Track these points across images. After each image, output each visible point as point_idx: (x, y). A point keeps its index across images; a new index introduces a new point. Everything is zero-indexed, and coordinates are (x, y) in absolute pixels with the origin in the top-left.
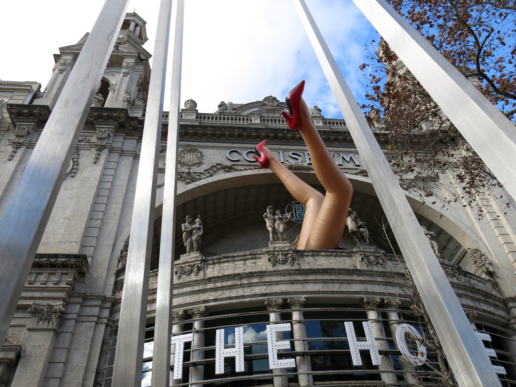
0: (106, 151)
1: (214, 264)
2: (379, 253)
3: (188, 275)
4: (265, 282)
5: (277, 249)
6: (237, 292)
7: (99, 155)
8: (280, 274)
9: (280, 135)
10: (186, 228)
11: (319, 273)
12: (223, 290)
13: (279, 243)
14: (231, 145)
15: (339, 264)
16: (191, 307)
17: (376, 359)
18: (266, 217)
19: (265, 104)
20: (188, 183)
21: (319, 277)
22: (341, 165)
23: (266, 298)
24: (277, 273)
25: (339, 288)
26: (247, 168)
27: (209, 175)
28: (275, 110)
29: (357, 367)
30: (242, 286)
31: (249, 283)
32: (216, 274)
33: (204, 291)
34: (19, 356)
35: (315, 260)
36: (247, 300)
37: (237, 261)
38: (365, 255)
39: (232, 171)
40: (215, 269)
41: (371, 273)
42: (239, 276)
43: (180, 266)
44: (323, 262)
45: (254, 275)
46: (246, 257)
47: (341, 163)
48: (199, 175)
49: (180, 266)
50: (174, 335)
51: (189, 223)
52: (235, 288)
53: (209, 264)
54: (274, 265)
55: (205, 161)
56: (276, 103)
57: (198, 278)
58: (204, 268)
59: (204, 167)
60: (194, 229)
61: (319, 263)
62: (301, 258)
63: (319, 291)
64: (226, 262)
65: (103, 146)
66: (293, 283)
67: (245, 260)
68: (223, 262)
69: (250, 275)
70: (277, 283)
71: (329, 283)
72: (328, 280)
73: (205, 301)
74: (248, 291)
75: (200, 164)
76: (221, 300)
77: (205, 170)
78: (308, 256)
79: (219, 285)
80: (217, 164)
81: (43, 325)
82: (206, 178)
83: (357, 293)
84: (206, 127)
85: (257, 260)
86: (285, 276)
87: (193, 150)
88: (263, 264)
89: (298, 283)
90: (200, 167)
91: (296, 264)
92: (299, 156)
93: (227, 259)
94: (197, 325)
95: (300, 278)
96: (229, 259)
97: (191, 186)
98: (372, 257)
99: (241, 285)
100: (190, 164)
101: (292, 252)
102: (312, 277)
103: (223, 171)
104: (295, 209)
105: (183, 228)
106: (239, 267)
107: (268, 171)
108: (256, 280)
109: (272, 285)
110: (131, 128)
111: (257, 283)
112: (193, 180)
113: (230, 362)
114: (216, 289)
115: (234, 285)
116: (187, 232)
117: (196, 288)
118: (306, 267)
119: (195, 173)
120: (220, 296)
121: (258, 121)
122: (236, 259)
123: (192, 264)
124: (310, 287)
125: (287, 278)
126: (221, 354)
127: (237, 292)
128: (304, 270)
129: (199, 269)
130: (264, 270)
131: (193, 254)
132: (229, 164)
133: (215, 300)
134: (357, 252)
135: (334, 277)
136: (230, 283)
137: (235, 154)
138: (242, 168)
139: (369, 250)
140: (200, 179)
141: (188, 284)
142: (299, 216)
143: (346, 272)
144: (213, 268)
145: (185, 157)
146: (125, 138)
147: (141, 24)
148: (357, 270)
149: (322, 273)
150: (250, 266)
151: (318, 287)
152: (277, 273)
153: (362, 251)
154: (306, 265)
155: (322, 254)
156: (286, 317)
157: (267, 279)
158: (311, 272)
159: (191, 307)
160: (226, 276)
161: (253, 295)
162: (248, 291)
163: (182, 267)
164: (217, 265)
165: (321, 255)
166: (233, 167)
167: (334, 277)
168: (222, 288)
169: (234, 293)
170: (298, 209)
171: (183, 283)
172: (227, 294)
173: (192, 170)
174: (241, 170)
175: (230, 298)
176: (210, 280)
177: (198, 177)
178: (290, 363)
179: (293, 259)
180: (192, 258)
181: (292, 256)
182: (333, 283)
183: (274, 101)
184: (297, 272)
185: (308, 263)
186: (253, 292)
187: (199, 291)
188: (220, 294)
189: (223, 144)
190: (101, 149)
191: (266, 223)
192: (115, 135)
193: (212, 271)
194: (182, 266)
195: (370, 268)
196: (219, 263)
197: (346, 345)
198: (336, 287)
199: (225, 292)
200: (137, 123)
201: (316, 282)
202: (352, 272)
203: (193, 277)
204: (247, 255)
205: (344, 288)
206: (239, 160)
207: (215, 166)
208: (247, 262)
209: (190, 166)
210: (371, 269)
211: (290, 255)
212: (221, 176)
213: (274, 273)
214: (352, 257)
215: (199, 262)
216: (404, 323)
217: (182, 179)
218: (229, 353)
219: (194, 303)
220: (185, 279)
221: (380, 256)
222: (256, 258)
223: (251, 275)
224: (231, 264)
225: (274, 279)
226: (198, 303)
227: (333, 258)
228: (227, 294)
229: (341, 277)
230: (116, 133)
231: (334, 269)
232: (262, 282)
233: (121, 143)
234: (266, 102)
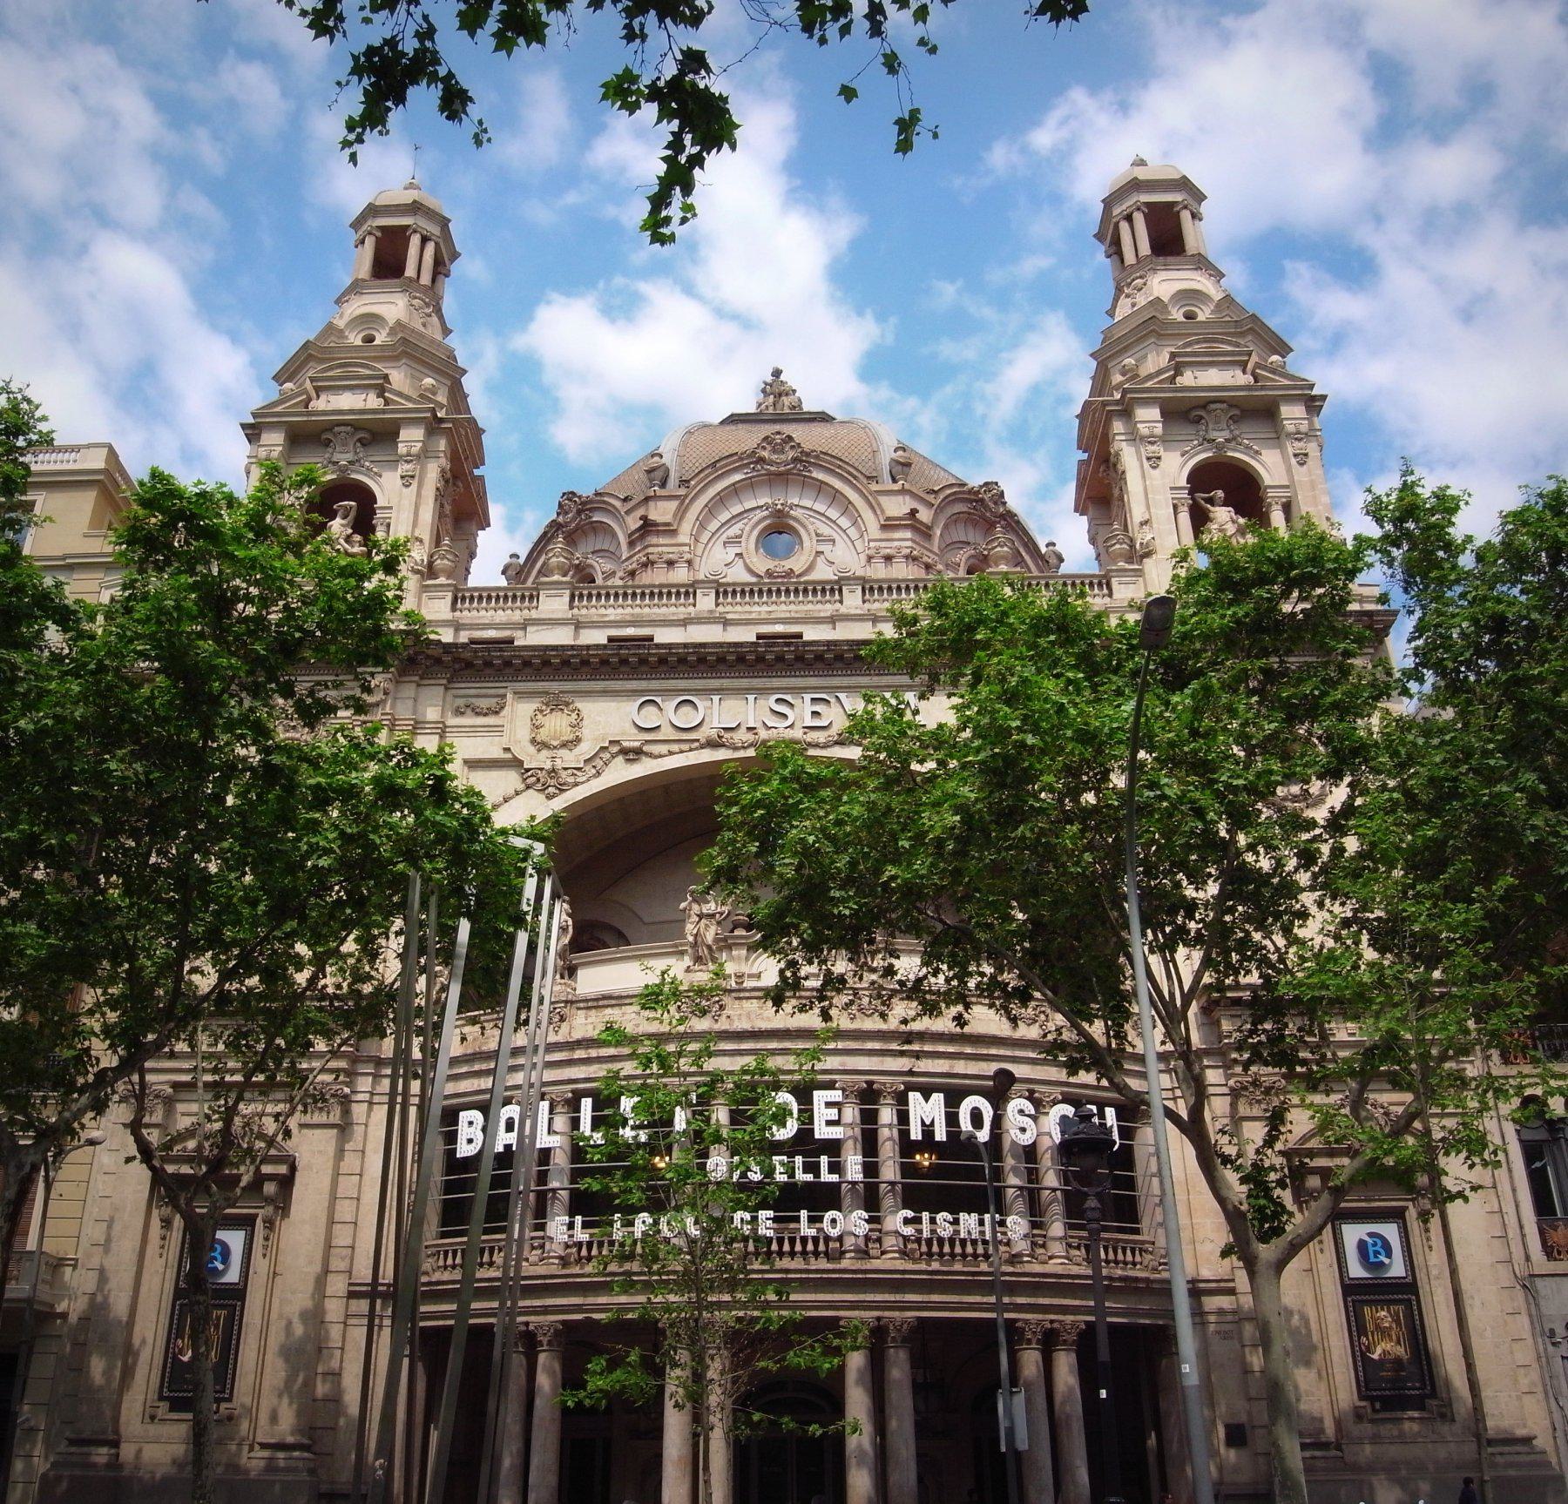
14: (643, 685)
19: (762, 460)
20: (550, 797)
26: (675, 747)
28: (788, 473)
34: (293, 1169)
59: (586, 749)
79: (593, 1053)
81: (319, 1118)
90: (577, 750)
91: (723, 1018)
97: (560, 803)
103: (620, 758)
129: (562, 1019)
137: (651, 709)
138: (663, 749)
140: (576, 784)
147: (434, 229)
166: (645, 748)
173: (559, 764)
212: (620, 773)
217: (539, 786)
233: (410, 703)
234: (765, 454)
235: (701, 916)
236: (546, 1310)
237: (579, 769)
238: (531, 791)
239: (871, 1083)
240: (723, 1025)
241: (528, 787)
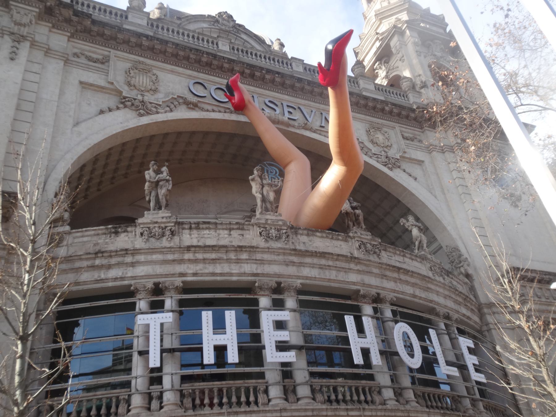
0: (28, 44)
1: (190, 228)
2: (376, 241)
3: (158, 239)
4: (256, 260)
6: (222, 267)
7: (17, 49)
8: (274, 252)
9: (258, 74)
10: (150, 177)
11: (316, 256)
12: (205, 263)
13: (270, 214)
14: (195, 74)
15: (336, 249)
16: (163, 280)
17: (376, 359)
18: (253, 180)
20: (141, 115)
21: (315, 261)
22: (323, 127)
23: (257, 279)
24: (270, 250)
25: (336, 276)
27: (168, 109)
29: (357, 366)
31: (238, 259)
32: (195, 242)
33: (181, 261)
35: (311, 241)
36: (235, 278)
37: (219, 229)
39: (197, 109)
40: (193, 236)
41: (368, 263)
42: (225, 249)
43: (145, 226)
44: (320, 243)
45: (244, 250)
46: (232, 226)
47: (323, 125)
48: (155, 107)
49: (145, 226)
50: (142, 313)
51: (154, 171)
52: (220, 263)
53: (183, 229)
54: (266, 241)
55: (161, 89)
56: (232, 24)
57: (172, 244)
58: (179, 233)
60: (161, 180)
61: (315, 245)
62: (294, 236)
63: (315, 278)
64: (207, 228)
65: (22, 36)
66: (287, 265)
67: (230, 230)
68: (203, 229)
69: (238, 249)
70: (270, 262)
71: (326, 269)
72: (325, 265)
73: (182, 274)
74: (235, 269)
75: (155, 91)
76: (202, 275)
77: (163, 102)
78: (302, 234)
79: (200, 256)
80: (178, 96)
82: (166, 112)
83: (354, 283)
84: (167, 42)
86: (278, 255)
87: (146, 71)
88: (252, 237)
89: (293, 265)
90: (156, 96)
92: (277, 105)
93: (207, 226)
94: (168, 303)
95: (295, 259)
96: (211, 226)
97: (145, 120)
98: (369, 245)
99: (227, 259)
100: (143, 89)
102: (308, 260)
103: (184, 107)
105: (147, 177)
106: (223, 237)
107: (242, 118)
109: (263, 264)
110: (60, 18)
111: (246, 259)
112: (148, 113)
113: (220, 350)
114: (196, 261)
115: (218, 259)
116: (152, 182)
117: (170, 257)
118: (301, 247)
119: (151, 103)
120: (201, 270)
121: (227, 48)
122: (219, 227)
123: (163, 225)
125: (281, 258)
126: (209, 340)
128: (300, 251)
129: (173, 233)
131: (162, 213)
132: (195, 100)
133: (195, 274)
134: (354, 237)
135: (330, 263)
136: (213, 256)
137: (200, 87)
138: (210, 108)
139: (366, 237)
140: (158, 113)
141: (159, 250)
143: (344, 258)
144: (190, 235)
145: (136, 78)
146: (50, 31)
148: (355, 258)
149: (320, 256)
150: (234, 238)
153: (359, 237)
154: (302, 245)
155: (318, 234)
156: (278, 305)
157: (259, 256)
158: (308, 254)
159: (163, 280)
160: (209, 246)
161: (242, 273)
162: (235, 269)
163: (149, 228)
164: (195, 232)
165: (316, 236)
166: (199, 105)
167: (330, 263)
169: (218, 269)
170: (271, 172)
171: (152, 249)
172: (210, 268)
173: (146, 99)
174: (208, 111)
175: (213, 274)
176: (188, 248)
177: (154, 110)
178: (289, 356)
179: (288, 236)
180: (163, 218)
181: (286, 233)
182: (330, 269)
183: (230, 20)
184: (293, 252)
185: (304, 243)
186: (242, 271)
187: (174, 261)
189: (184, 70)
190: (19, 39)
191: (251, 187)
192: (36, 23)
193: (189, 238)
194: (148, 226)
195: (366, 257)
196: (198, 228)
197: (346, 340)
198: (332, 275)
199: (207, 266)
200: (71, 13)
201: (312, 266)
202: (350, 259)
203: (165, 243)
204: (233, 224)
205: (341, 276)
206: (205, 97)
207: (175, 99)
208: (232, 232)
209: (142, 91)
210: (368, 258)
211: (284, 231)
212: (182, 114)
214: (348, 242)
215: (173, 224)
216: (402, 321)
218: (220, 340)
219: (166, 276)
220: (154, 243)
221: (376, 245)
222: (243, 229)
223: (240, 248)
224: (212, 232)
226: (173, 275)
227: (329, 240)
228: (210, 268)
229: (338, 264)
230: (39, 20)
231: (332, 254)
232: (253, 259)
237: (160, 105)
238: (127, 109)
241: (125, 107)
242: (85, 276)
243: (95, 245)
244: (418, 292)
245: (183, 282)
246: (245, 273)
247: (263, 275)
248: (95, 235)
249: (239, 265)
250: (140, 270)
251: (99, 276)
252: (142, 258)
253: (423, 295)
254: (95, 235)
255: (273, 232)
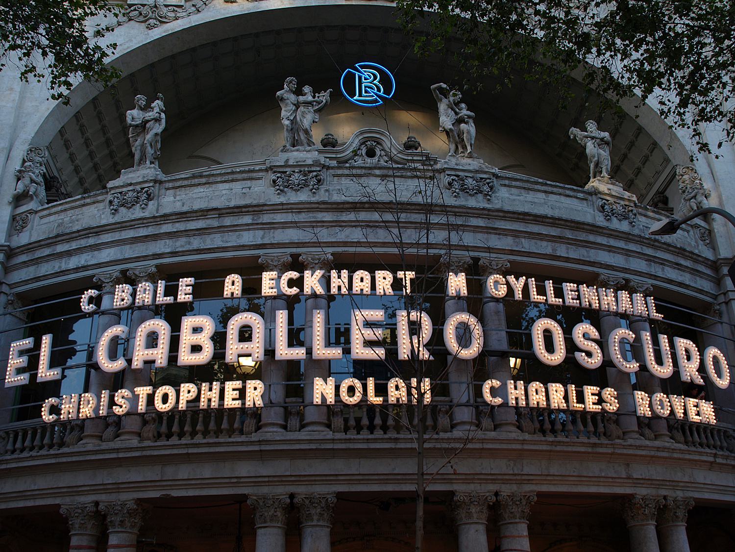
5: (291, 163)
6: (212, 240)
20: (150, 27)
24: (285, 207)
30: (221, 229)
33: (155, 237)
38: (457, 176)
40: (178, 198)
48: (174, 11)
57: (147, 214)
70: (284, 225)
85: (254, 182)
91: (322, 191)
97: (158, 33)
98: (470, 180)
101: (318, 169)
104: (360, 78)
108: (247, 219)
109: (274, 228)
117: (143, 232)
119: (166, 6)
120: (182, 246)
124: (342, 235)
127: (212, 240)
129: (149, 198)
130: (262, 201)
133: (174, 254)
142: (366, 92)
151: (356, 235)
152: (285, 207)
157: (266, 218)
162: (232, 240)
168: (187, 233)
170: (366, 79)
176: (166, 218)
177: (173, 15)
188: (183, 243)
194: (120, 190)
201: (355, 224)
203: (137, 213)
210: (463, 203)
213: (280, 207)
225: (280, 218)
228: (196, 243)
232: (257, 224)
235: (297, 106)
236: (118, 487)
238: (132, 22)
239: (476, 260)
240: (322, 196)
242: (45, 269)
243: (59, 226)
244: (562, 251)
245: (157, 266)
246: (243, 246)
247: (272, 246)
248: (62, 211)
249: (237, 233)
250: (106, 255)
251: (60, 267)
252: (106, 238)
253: (574, 253)
254: (62, 211)
255: (296, 178)
